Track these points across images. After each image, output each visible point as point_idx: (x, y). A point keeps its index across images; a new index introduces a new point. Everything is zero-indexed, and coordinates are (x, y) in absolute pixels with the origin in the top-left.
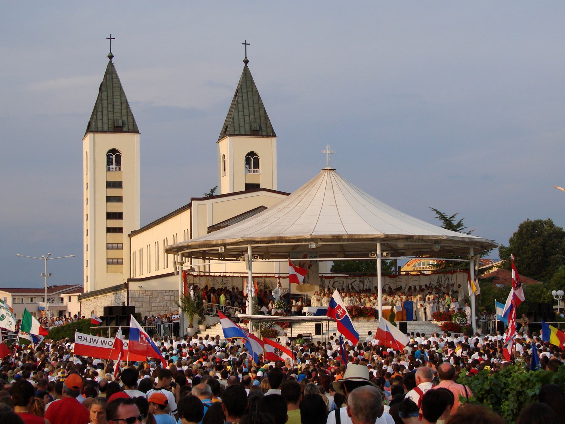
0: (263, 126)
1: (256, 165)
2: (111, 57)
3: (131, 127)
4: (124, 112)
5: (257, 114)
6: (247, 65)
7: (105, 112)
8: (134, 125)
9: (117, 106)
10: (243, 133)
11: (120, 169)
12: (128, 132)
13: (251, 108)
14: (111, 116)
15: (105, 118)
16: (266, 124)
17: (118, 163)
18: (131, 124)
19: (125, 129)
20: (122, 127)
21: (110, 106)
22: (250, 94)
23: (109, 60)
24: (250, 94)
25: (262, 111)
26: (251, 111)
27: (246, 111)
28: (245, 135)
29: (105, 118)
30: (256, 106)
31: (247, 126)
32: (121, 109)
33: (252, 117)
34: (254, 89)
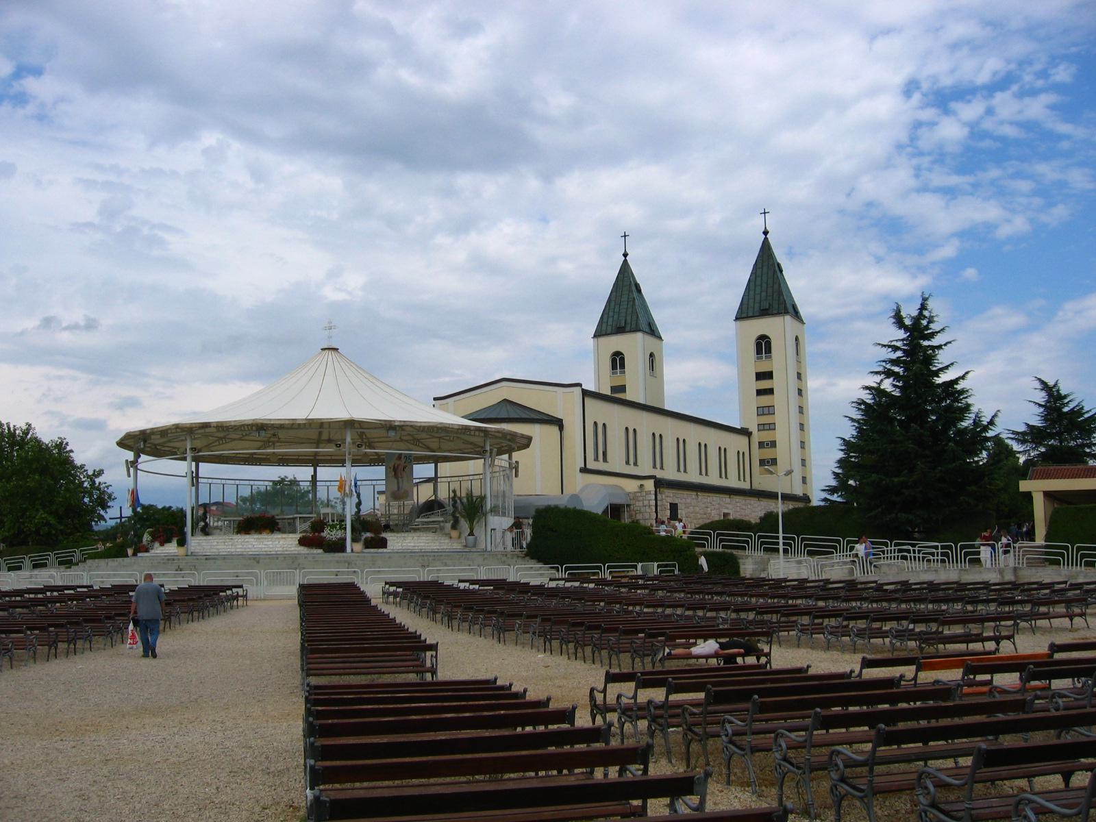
0: (776, 306)
1: (769, 350)
2: (625, 255)
3: (634, 326)
4: (630, 310)
5: (770, 290)
6: (768, 236)
7: (611, 314)
8: (637, 324)
9: (624, 306)
10: (750, 314)
11: (624, 372)
12: (630, 331)
13: (764, 285)
14: (616, 317)
15: (610, 319)
16: (779, 300)
17: (623, 366)
18: (634, 322)
19: (628, 328)
20: (624, 327)
21: (617, 307)
22: (765, 268)
23: (624, 258)
24: (765, 268)
25: (776, 286)
26: (764, 288)
27: (758, 289)
28: (753, 317)
29: (610, 319)
30: (770, 282)
31: (757, 306)
32: (627, 309)
33: (764, 294)
34: (771, 263)
